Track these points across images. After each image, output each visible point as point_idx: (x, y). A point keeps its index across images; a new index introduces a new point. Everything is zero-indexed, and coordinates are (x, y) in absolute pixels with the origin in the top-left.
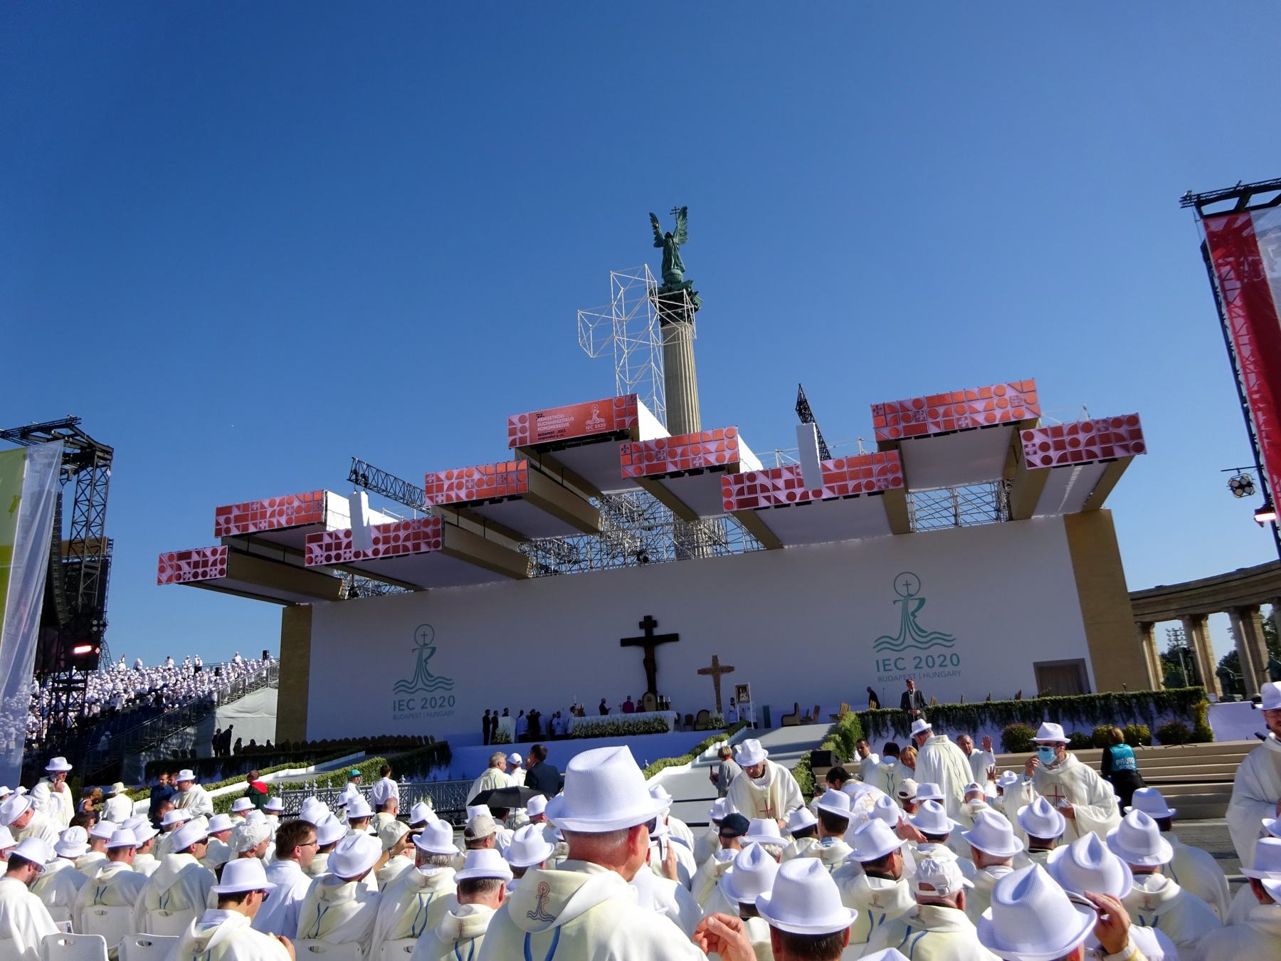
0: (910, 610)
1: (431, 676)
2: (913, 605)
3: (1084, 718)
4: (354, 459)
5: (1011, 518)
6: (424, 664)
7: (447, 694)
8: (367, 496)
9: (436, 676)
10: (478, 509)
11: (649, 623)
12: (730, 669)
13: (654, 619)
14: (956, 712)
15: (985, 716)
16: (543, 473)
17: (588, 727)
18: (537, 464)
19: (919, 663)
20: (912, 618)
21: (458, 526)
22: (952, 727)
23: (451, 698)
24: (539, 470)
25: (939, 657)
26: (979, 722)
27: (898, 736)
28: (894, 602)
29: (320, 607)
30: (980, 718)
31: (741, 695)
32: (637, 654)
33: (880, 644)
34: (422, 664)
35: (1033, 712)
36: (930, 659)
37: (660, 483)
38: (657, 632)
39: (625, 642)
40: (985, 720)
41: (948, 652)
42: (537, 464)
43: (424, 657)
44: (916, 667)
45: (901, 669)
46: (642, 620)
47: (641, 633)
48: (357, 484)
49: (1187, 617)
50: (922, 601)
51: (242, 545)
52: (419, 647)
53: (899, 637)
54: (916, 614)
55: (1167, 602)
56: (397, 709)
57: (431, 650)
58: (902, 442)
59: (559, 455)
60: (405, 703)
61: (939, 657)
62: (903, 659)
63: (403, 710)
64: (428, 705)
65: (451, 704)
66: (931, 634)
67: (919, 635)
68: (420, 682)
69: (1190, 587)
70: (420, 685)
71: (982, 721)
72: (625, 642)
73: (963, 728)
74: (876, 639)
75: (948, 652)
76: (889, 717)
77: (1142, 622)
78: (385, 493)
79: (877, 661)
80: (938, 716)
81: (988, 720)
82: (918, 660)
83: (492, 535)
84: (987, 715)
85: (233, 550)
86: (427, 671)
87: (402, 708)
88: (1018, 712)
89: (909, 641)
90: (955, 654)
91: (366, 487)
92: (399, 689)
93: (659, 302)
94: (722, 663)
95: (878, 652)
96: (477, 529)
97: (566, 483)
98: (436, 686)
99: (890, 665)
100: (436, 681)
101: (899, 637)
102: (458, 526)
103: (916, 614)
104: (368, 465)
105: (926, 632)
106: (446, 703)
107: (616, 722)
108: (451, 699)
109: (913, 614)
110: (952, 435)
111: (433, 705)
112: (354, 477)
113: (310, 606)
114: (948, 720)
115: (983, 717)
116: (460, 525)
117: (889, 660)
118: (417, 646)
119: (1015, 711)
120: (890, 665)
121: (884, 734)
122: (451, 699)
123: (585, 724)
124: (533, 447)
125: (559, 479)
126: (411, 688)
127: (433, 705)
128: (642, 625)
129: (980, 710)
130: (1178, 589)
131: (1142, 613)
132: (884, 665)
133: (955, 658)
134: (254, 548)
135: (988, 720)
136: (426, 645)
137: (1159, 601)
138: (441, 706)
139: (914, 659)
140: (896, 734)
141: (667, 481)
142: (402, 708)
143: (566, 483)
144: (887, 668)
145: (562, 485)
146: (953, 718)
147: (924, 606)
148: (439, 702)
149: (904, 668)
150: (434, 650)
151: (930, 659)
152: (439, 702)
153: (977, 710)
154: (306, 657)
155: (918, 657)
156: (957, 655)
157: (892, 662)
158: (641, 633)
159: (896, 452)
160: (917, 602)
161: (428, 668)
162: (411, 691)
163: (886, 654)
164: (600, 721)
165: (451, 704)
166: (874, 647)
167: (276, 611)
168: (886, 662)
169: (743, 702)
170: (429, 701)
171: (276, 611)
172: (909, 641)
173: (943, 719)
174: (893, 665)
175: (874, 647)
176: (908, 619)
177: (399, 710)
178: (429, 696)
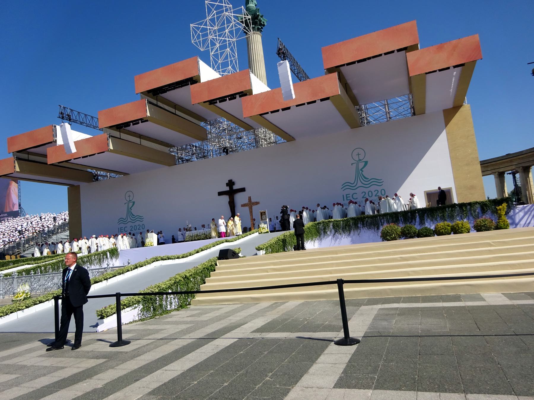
0: (360, 168)
1: (134, 216)
2: (361, 165)
3: (439, 219)
4: (60, 106)
5: (414, 114)
6: (130, 210)
7: (141, 223)
8: (69, 126)
9: (136, 215)
10: (128, 128)
11: (231, 183)
12: (257, 203)
13: (233, 181)
14: (368, 219)
15: (384, 220)
16: (161, 107)
17: (193, 236)
18: (155, 102)
19: (364, 196)
20: (361, 172)
21: (120, 139)
22: (366, 228)
23: (143, 225)
24: (157, 106)
25: (375, 191)
26: (381, 224)
27: (336, 233)
28: (352, 164)
29: (83, 186)
30: (381, 223)
31: (263, 216)
32: (226, 199)
33: (343, 187)
34: (129, 210)
35: (410, 217)
36: (370, 193)
37: (216, 106)
38: (235, 187)
39: (220, 194)
40: (384, 223)
41: (379, 188)
42: (155, 102)
43: (130, 206)
44: (363, 197)
45: (355, 199)
46: (227, 182)
47: (227, 189)
48: (63, 119)
49: (521, 168)
50: (366, 163)
51: (25, 156)
52: (127, 202)
53: (354, 182)
54: (363, 170)
55: (511, 161)
56: (120, 232)
57: (132, 203)
58: (341, 68)
59: (165, 95)
60: (123, 228)
61: (375, 191)
62: (356, 194)
63: (123, 232)
64: (133, 229)
65: (143, 228)
66: (372, 179)
67: (363, 180)
68: (129, 217)
69: (523, 153)
70: (129, 220)
71: (381, 223)
72: (220, 194)
73: (372, 228)
74: (343, 184)
75: (379, 188)
76: (331, 224)
77: (498, 172)
78: (97, 128)
79: (343, 195)
80: (358, 222)
81: (385, 222)
82: (364, 193)
83: (145, 143)
84: (385, 220)
85: (18, 159)
86: (132, 213)
87: (122, 231)
88: (402, 218)
89: (359, 184)
90: (382, 190)
91: (69, 121)
92: (119, 223)
93: (234, 16)
94: (253, 200)
95: (343, 191)
96: (136, 140)
97: (178, 113)
98: (137, 220)
99: (349, 197)
100: (136, 217)
101: (354, 182)
102: (120, 139)
103: (363, 170)
104: (72, 110)
105: (368, 179)
106: (141, 228)
107: (206, 234)
108: (143, 225)
109: (361, 170)
110: (367, 61)
111: (135, 229)
112: (61, 116)
113: (79, 186)
114: (363, 224)
115: (383, 221)
116: (121, 138)
117: (349, 194)
118: (126, 202)
119: (400, 217)
120: (349, 197)
121: (329, 233)
122: (143, 226)
123: (191, 235)
124: (149, 92)
125: (173, 110)
126: (125, 222)
127: (135, 229)
128: (227, 185)
129: (381, 218)
130: (517, 155)
131: (498, 167)
132: (347, 197)
133: (383, 191)
134: (32, 157)
135: (385, 222)
136: (130, 201)
137: (508, 161)
138: (139, 229)
139: (362, 193)
140: (335, 232)
141: (218, 104)
142: (122, 231)
143: (178, 113)
144: (348, 198)
145: (175, 114)
146: (366, 222)
147: (367, 166)
148: (138, 228)
149: (357, 198)
150: (134, 202)
151: (370, 193)
152: (138, 228)
153: (380, 217)
154: (79, 209)
155: (364, 192)
156: (384, 190)
157: (351, 196)
158: (227, 189)
159: (335, 75)
160: (364, 163)
161: (132, 212)
162: (125, 223)
163: (348, 191)
164: (198, 233)
165: (143, 228)
166: (342, 188)
167: (65, 188)
168: (348, 196)
169: (264, 219)
170: (133, 227)
171: (65, 188)
172: (359, 184)
173: (361, 223)
174: (351, 197)
175: (342, 188)
176: (359, 173)
177: (121, 232)
178: (133, 225)
